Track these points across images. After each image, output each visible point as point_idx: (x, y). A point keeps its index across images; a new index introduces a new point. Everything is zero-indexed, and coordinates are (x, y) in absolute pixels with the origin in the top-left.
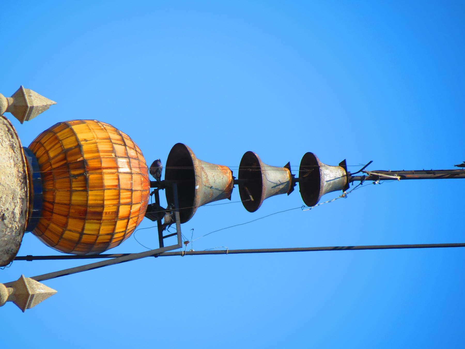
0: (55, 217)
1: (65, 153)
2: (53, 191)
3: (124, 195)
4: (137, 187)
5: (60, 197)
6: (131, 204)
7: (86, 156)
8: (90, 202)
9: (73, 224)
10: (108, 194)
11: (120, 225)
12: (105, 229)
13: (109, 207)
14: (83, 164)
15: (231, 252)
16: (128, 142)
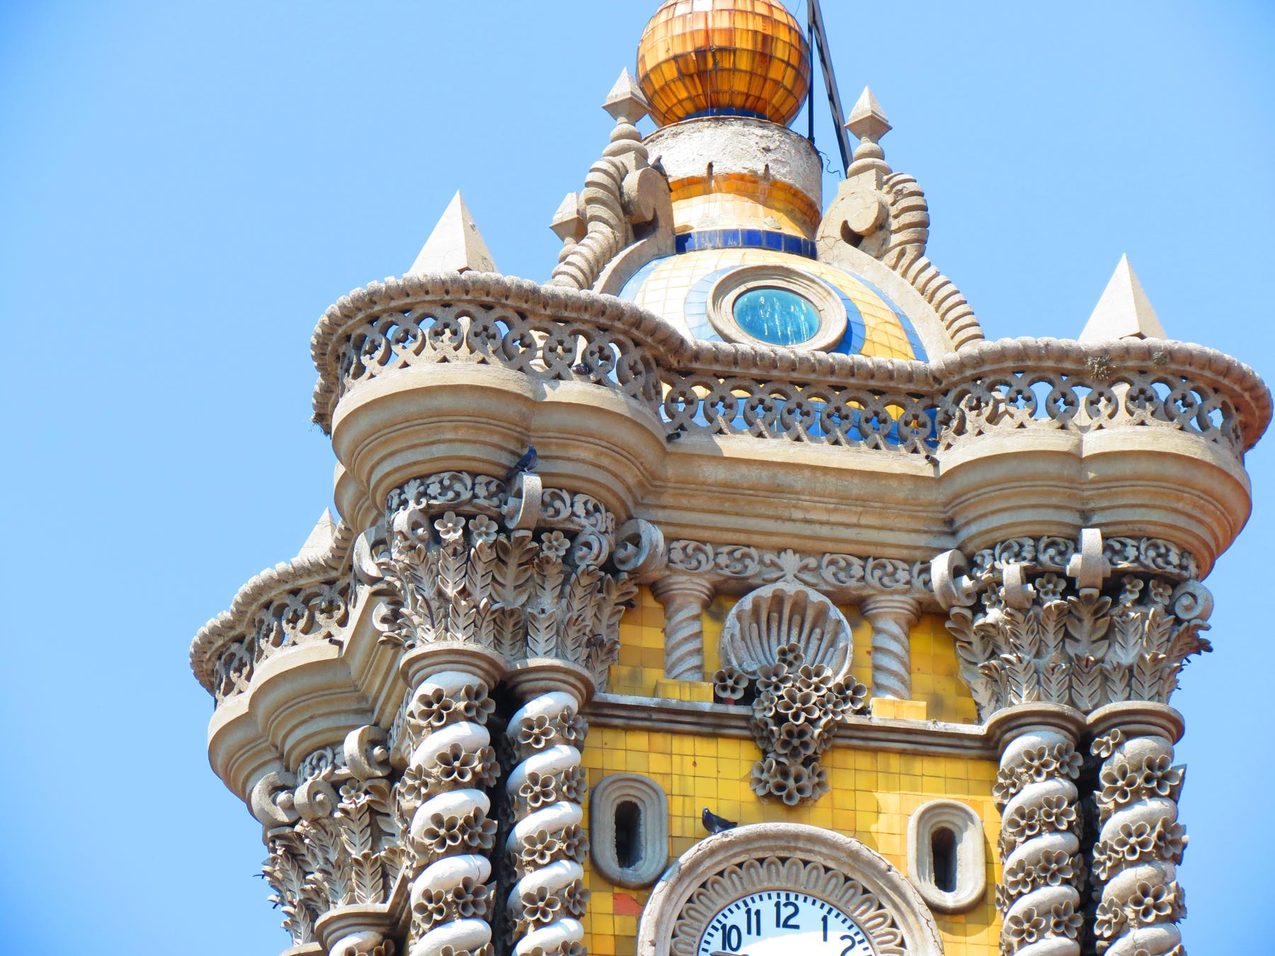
0: (765, 95)
1: (683, 76)
5: (740, 85)
7: (690, 48)
8: (750, 47)
9: (776, 72)
10: (740, 23)
11: (777, 15)
12: (783, 35)
13: (759, 25)
14: (701, 53)
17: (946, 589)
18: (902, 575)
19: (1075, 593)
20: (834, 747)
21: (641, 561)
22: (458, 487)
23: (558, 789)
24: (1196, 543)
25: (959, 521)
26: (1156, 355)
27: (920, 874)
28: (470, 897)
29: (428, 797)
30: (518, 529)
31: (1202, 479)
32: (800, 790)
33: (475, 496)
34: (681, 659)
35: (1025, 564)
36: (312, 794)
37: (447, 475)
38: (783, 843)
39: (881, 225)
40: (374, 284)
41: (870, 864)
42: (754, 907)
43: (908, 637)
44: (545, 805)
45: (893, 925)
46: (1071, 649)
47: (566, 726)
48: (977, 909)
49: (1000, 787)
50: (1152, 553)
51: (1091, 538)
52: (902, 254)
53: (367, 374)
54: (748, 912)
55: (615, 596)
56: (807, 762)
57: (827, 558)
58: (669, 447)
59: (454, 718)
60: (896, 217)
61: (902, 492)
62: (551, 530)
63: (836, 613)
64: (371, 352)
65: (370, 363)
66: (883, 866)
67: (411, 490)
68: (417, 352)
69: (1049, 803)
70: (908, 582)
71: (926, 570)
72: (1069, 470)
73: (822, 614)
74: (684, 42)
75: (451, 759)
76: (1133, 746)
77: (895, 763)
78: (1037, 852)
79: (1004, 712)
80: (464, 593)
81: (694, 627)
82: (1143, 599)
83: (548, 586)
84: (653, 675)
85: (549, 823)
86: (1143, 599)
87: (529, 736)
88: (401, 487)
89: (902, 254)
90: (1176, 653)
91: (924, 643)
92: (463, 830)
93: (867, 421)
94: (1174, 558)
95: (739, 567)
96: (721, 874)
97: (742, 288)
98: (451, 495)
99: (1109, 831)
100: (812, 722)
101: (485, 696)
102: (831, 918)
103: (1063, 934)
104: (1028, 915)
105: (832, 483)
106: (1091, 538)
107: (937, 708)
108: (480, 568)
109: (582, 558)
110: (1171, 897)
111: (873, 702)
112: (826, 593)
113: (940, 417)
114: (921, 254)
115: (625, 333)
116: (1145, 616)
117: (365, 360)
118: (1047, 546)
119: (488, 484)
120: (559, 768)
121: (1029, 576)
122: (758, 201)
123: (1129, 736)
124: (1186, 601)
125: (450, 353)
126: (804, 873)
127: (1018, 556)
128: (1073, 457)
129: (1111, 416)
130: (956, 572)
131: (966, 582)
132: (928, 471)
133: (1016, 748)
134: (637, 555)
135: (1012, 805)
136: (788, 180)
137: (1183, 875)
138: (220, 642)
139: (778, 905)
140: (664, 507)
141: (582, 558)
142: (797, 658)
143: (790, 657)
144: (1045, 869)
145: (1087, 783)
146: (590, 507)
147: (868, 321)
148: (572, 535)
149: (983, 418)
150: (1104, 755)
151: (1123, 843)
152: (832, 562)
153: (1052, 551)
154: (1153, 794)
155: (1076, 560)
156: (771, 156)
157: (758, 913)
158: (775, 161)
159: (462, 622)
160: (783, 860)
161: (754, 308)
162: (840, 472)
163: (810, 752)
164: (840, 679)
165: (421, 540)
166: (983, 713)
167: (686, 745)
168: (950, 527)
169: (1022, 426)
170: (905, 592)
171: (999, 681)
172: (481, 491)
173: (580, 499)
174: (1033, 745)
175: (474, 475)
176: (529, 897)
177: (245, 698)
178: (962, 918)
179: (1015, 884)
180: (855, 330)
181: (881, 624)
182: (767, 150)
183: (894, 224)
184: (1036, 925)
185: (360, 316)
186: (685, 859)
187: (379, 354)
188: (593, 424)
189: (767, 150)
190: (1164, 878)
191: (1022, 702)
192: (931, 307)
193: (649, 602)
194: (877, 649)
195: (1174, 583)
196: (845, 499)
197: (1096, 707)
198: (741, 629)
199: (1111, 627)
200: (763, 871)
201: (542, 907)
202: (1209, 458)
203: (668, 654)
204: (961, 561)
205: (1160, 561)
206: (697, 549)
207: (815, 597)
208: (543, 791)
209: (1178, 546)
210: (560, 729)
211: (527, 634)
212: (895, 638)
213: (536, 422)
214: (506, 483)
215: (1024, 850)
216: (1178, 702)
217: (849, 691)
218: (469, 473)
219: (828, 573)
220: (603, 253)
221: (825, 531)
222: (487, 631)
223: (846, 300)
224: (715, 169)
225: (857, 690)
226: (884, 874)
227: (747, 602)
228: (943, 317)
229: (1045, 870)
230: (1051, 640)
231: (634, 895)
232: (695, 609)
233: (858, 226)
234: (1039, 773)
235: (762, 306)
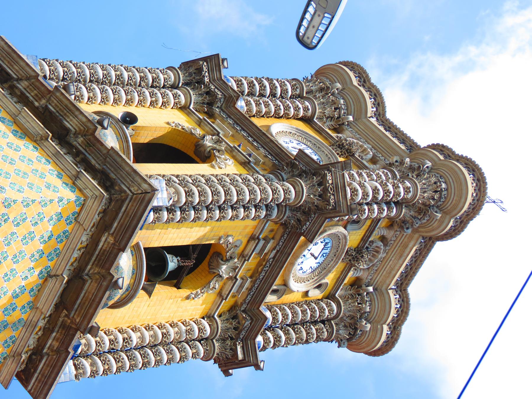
102: (319, 264)
126: (330, 259)
160: (335, 255)
200: (335, 251)
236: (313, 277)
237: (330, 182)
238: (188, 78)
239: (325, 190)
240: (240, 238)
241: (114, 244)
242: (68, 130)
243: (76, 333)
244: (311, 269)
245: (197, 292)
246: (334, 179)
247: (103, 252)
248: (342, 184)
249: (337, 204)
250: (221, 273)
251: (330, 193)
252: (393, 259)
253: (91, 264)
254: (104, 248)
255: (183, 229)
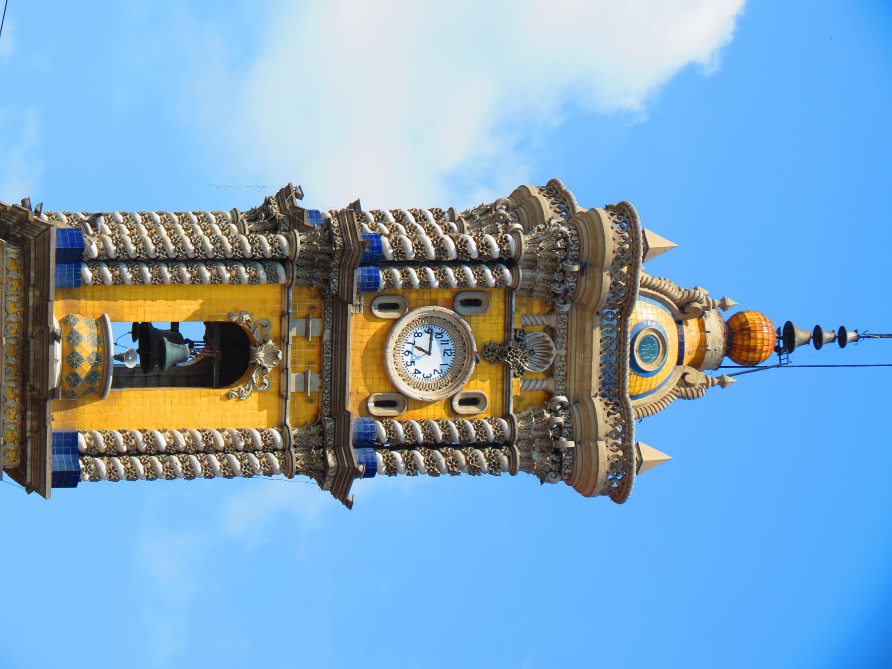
0: (737, 351)
1: (741, 324)
2: (736, 340)
3: (765, 342)
4: (771, 339)
5: (739, 342)
6: (768, 346)
7: (750, 326)
8: (752, 345)
9: (744, 354)
10: (759, 341)
11: (763, 354)
12: (757, 356)
13: (759, 348)
14: (749, 329)
15: (809, 366)
16: (767, 320)
17: (555, 400)
18: (561, 388)
19: (554, 440)
20: (503, 367)
21: (558, 304)
22: (575, 246)
23: (480, 279)
24: (573, 478)
25: (578, 405)
26: (630, 463)
27: (463, 394)
28: (442, 252)
29: (474, 239)
30: (562, 265)
31: (592, 479)
32: (488, 356)
33: (572, 251)
34: (529, 319)
35: (563, 424)
36: (503, 215)
37: (578, 242)
38: (470, 351)
39: (687, 385)
40: (638, 217)
41: (464, 378)
42: (449, 342)
43: (542, 390)
44: (475, 275)
45: (446, 386)
46: (537, 440)
47: (501, 282)
48: (453, 413)
49: (492, 418)
50: (568, 464)
51: (572, 444)
52: (677, 391)
53: (611, 217)
54: (448, 341)
55: (548, 297)
56: (497, 358)
57: (565, 364)
58: (595, 312)
59: (500, 246)
60: (691, 390)
61: (586, 386)
62: (564, 275)
63: (547, 367)
64: (618, 218)
65: (614, 218)
66: (464, 382)
67: (574, 232)
68: (617, 232)
69: (486, 433)
70: (559, 390)
71: (563, 395)
72: (593, 437)
73: (547, 362)
74: (752, 324)
75: (487, 246)
76: (505, 458)
77: (500, 386)
78: (470, 429)
79: (516, 419)
80: (541, 249)
81: (540, 323)
82: (554, 462)
83: (546, 275)
84: (524, 310)
85: (469, 276)
86: (554, 462)
87: (497, 270)
88: (576, 229)
89: (677, 391)
90: (538, 473)
91: (541, 395)
92: (463, 249)
93: (609, 375)
94: (567, 471)
95: (560, 336)
96: (459, 332)
97: (658, 339)
98: (572, 244)
99: (479, 452)
100: (509, 359)
101: (509, 256)
102: (448, 366)
103: (443, 437)
104: (448, 426)
105: (587, 364)
106: (572, 444)
107: (518, 399)
108: (549, 254)
109: (555, 285)
110: (456, 470)
111: (519, 379)
112: (553, 363)
113: (612, 398)
114: (678, 397)
115: (628, 297)
116: (548, 462)
117: (616, 216)
118: (569, 431)
119: (576, 255)
120: (487, 279)
121: (559, 425)
122: (698, 348)
123: (509, 458)
124: (553, 475)
125: (616, 242)
126: (461, 357)
127: (566, 422)
128: (597, 439)
129: (611, 450)
130: (562, 403)
131: (558, 407)
132: (593, 394)
133: (504, 423)
134: (560, 303)
135: (486, 422)
136: (706, 357)
137: (464, 476)
138: (556, 187)
139: (451, 350)
140: (577, 311)
141: (555, 285)
142: (532, 355)
143: (532, 352)
144: (464, 431)
145: (496, 445)
146: (572, 287)
147: (650, 379)
148: (563, 282)
149: (609, 410)
150: (503, 450)
151: (473, 455)
152: (564, 365)
153: (568, 433)
154: (489, 465)
155: (564, 440)
156: (714, 352)
157: (448, 344)
158: (712, 353)
159: (532, 248)
160: (465, 351)
161: (652, 342)
162: (591, 366)
163: (500, 359)
164: (525, 368)
165: (557, 235)
166: (517, 414)
167: (501, 321)
168: (576, 402)
169: (606, 422)
170: (555, 388)
171: (527, 418)
172: (574, 253)
173: (574, 284)
174: (505, 428)
175: (579, 251)
176: (444, 271)
177: (537, 195)
178: (450, 407)
179: (459, 422)
180: (645, 374)
181: (545, 381)
182: (716, 350)
183: (688, 389)
184: (445, 429)
185: (629, 214)
186: (463, 320)
187: (617, 220)
188: (597, 287)
189: (716, 350)
190: (461, 468)
191: (518, 425)
192: (659, 400)
193: (548, 309)
194: (537, 380)
195: (560, 472)
196: (583, 368)
197: (519, 448)
198: (539, 337)
199: (545, 452)
200: (461, 345)
201: (442, 275)
202: (599, 481)
203: (532, 315)
204: (566, 405)
205: (566, 466)
206: (565, 323)
207: (551, 360)
208: (480, 275)
209: (572, 472)
210: (500, 279)
211: (531, 269)
212: (541, 386)
213: (597, 269)
214: (576, 260)
215: (470, 425)
216: (521, 474)
217: (521, 371)
218: (579, 249)
219: (560, 364)
220: (670, 296)
221: (573, 362)
222: (528, 256)
223: (657, 371)
224: (708, 334)
225: (522, 374)
226: (462, 382)
227: (548, 338)
228: (655, 403)
229: (463, 431)
230: (540, 433)
231: (451, 305)
232: (546, 323)
233: (687, 378)
234: (496, 429)
235: (652, 345)
236: (445, 383)
237: (336, 225)
238: (253, 215)
239: (331, 235)
240: (263, 315)
241: (41, 296)
242: (8, 227)
243: (46, 402)
244: (437, 375)
245: (239, 389)
246: (341, 222)
247: (36, 308)
248: (351, 225)
249: (346, 244)
250: (259, 363)
251: (337, 236)
252: (577, 354)
253: (30, 324)
254: (35, 304)
255: (161, 303)
